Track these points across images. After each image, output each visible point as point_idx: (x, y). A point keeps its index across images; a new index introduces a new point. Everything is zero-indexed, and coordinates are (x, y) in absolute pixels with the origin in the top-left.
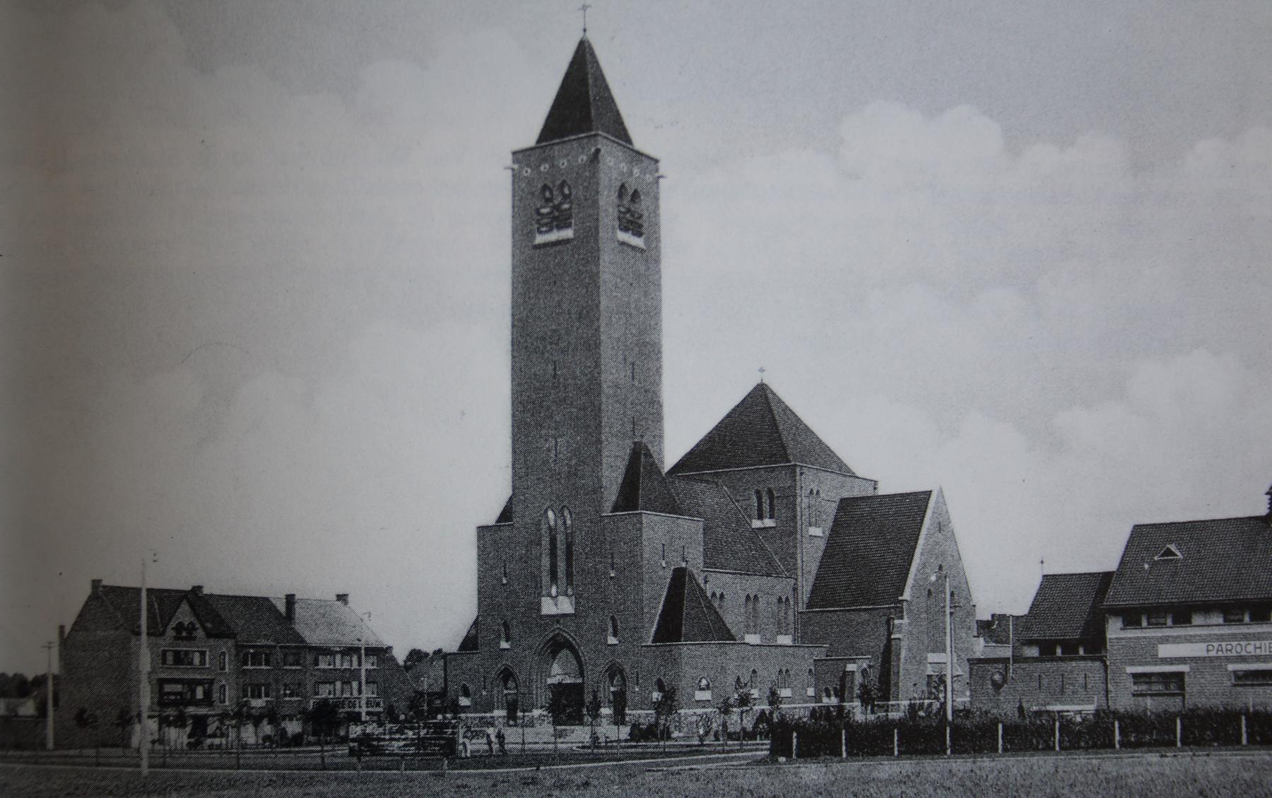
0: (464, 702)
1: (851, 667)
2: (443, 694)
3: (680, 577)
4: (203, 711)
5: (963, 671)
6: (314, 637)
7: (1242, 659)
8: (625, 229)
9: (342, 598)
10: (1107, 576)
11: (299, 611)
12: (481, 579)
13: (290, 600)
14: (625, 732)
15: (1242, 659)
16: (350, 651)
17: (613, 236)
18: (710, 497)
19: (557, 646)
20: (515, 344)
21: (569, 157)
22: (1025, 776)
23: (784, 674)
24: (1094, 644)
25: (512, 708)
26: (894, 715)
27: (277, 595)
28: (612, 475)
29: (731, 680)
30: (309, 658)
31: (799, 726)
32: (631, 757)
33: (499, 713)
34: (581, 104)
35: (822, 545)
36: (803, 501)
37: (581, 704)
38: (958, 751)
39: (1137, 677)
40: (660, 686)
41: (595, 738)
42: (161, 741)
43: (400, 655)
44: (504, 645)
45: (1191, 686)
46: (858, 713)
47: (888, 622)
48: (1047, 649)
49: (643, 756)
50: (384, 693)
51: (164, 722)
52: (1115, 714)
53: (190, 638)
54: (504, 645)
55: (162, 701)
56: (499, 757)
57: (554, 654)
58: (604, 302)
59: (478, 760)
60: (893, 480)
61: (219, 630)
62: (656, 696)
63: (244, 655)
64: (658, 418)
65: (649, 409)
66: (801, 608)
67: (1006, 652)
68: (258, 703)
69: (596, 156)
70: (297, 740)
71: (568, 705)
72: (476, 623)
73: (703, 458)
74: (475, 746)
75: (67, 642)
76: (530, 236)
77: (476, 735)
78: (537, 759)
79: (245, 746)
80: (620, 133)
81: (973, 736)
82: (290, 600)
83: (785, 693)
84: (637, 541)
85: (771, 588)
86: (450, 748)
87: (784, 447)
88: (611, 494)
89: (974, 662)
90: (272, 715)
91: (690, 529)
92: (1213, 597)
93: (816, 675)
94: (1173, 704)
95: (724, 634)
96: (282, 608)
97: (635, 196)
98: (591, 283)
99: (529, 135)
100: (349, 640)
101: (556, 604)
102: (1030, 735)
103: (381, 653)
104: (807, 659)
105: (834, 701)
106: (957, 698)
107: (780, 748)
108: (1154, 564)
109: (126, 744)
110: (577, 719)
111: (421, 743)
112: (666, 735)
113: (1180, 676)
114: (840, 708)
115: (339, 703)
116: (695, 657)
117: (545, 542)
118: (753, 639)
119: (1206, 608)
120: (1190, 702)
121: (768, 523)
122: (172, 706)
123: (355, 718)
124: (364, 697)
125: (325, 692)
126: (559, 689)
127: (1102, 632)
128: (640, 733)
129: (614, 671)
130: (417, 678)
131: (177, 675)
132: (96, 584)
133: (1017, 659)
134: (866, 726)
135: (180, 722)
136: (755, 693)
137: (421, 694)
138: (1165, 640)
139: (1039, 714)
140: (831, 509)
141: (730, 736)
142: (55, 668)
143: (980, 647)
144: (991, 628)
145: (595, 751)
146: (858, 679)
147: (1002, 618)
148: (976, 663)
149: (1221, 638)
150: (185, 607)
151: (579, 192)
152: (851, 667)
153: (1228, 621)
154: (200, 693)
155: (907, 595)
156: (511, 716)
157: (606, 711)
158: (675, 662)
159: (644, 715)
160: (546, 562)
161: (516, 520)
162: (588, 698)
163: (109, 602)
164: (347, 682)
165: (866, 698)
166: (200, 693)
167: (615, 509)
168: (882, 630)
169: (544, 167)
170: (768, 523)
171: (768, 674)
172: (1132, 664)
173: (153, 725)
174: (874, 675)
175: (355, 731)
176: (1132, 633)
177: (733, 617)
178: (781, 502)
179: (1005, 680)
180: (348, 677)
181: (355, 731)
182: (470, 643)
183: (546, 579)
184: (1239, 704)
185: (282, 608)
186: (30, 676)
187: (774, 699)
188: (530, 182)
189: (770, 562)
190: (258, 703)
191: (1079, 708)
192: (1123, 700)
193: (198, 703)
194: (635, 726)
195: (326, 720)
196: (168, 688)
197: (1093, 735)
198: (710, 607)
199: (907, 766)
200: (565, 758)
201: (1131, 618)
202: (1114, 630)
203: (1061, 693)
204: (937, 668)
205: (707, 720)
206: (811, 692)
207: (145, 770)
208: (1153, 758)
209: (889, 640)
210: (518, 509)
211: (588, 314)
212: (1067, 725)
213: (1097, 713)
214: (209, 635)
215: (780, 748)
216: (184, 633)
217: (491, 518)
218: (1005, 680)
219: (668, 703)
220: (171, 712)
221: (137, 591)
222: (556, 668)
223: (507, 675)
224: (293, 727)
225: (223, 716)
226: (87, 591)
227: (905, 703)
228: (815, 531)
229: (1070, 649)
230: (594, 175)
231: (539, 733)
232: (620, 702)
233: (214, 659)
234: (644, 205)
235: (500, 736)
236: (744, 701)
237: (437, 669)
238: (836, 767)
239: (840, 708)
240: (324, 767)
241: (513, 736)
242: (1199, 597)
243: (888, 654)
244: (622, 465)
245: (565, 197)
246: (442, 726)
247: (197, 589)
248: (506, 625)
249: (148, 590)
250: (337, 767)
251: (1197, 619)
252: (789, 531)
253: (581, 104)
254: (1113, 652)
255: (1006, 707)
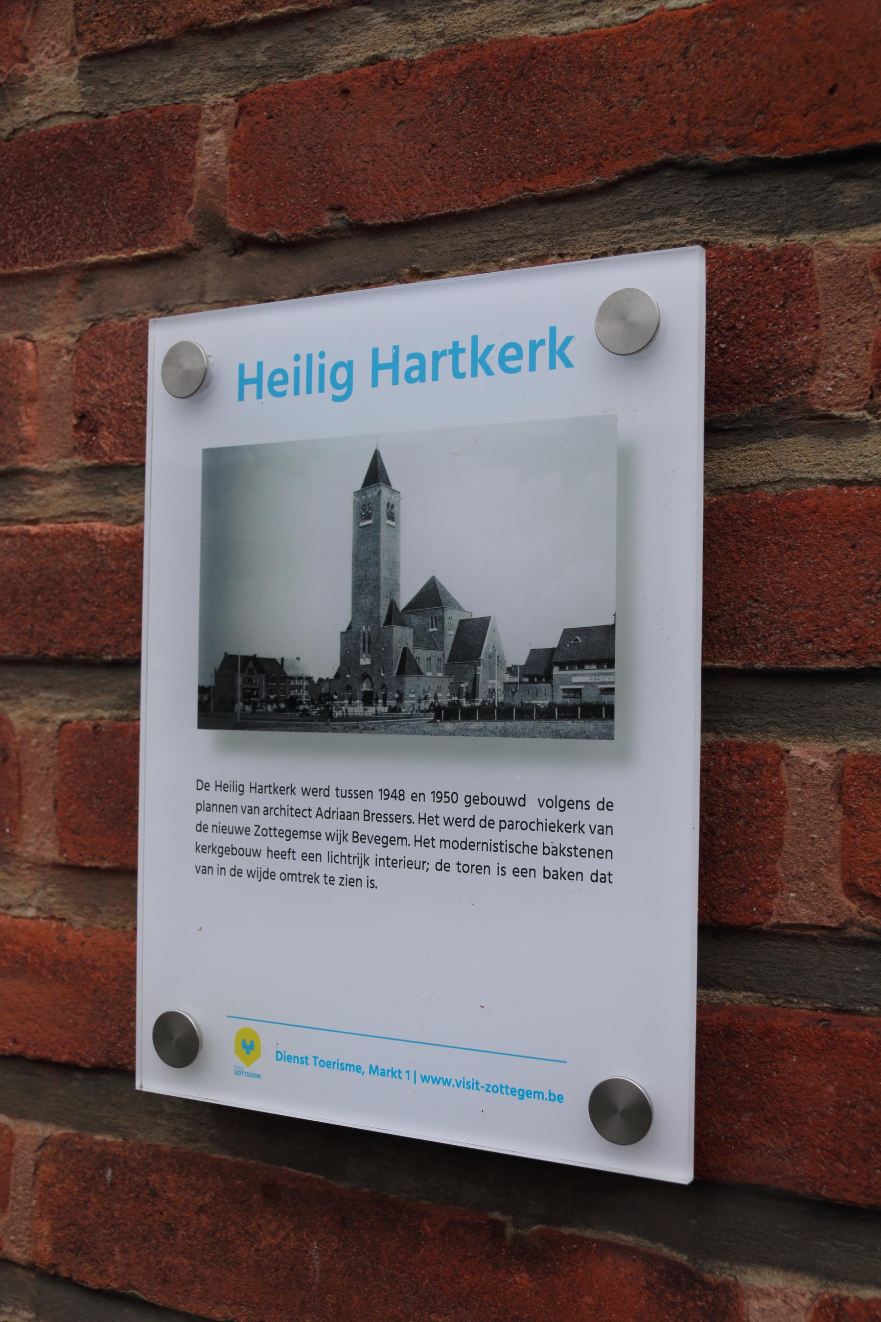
0: (335, 697)
1: (462, 685)
2: (329, 694)
3: (405, 650)
4: (256, 699)
5: (501, 687)
6: (290, 673)
7: (603, 683)
8: (389, 519)
9: (298, 659)
10: (553, 650)
11: (285, 664)
12: (341, 652)
13: (282, 659)
14: (386, 709)
15: (603, 683)
16: (300, 678)
17: (385, 521)
18: (416, 620)
19: (365, 677)
20: (353, 564)
21: (371, 493)
22: (523, 729)
23: (439, 688)
24: (548, 677)
25: (351, 699)
26: (477, 704)
27: (278, 658)
28: (383, 612)
29: (422, 690)
30: (288, 681)
31: (444, 708)
32: (388, 719)
33: (346, 701)
34: (376, 474)
35: (453, 638)
36: (446, 621)
37: (372, 698)
38: (499, 719)
39: (564, 690)
40: (398, 692)
41: (377, 711)
42: (244, 710)
43: (316, 680)
44: (348, 676)
45: (584, 695)
46: (465, 703)
47: (475, 668)
48: (531, 679)
49: (392, 718)
50: (310, 694)
51: (245, 703)
52: (556, 705)
53: (253, 673)
54: (348, 676)
55: (244, 695)
56: (346, 718)
57: (364, 680)
58: (382, 547)
59: (340, 719)
60: (476, 615)
61: (261, 671)
62: (397, 696)
63: (268, 681)
64: (398, 590)
65: (395, 587)
66: (446, 662)
67: (517, 680)
68: (272, 697)
69: (379, 493)
70: (284, 711)
71: (369, 699)
72: (339, 668)
73: (416, 605)
74: (338, 714)
75: (218, 674)
76: (358, 523)
77: (339, 709)
78: (358, 719)
79: (268, 712)
80: (388, 483)
81: (505, 713)
82: (282, 659)
83: (439, 695)
84: (391, 637)
85: (435, 654)
86: (330, 714)
87: (440, 600)
88: (383, 620)
89: (505, 684)
90: (277, 701)
91: (408, 632)
92: (593, 658)
93: (450, 688)
94: (577, 701)
95: (419, 672)
96: (280, 662)
97: (393, 506)
98: (377, 539)
99: (358, 486)
100: (300, 674)
101: (365, 661)
102: (525, 713)
103: (309, 679)
104: (447, 682)
105: (456, 698)
106: (499, 698)
107: (438, 717)
108: (571, 644)
109: (232, 710)
110: (370, 704)
111: (321, 712)
112: (400, 711)
113: (579, 691)
114: (458, 701)
115: (297, 697)
116: (410, 681)
117: (362, 638)
118: (429, 674)
119: (590, 662)
120: (584, 700)
121: (435, 629)
122: (247, 698)
123: (301, 703)
124: (304, 695)
125: (292, 693)
126: (365, 693)
127: (551, 671)
128: (392, 710)
129: (383, 686)
130: (321, 688)
131: (248, 686)
132: (226, 654)
133: (521, 682)
134: (467, 708)
135: (249, 703)
136: (430, 695)
137: (321, 694)
138: (575, 675)
139: (528, 704)
140: (456, 624)
141: (422, 711)
142: (213, 684)
143: (508, 678)
144: (511, 671)
145: (377, 717)
146: (465, 690)
147: (515, 666)
148: (506, 685)
149: (595, 674)
150: (251, 662)
151: (374, 506)
152: (462, 685)
153: (598, 668)
154: (255, 693)
155: (482, 657)
156: (350, 703)
157: (380, 701)
158: (402, 683)
159: (393, 703)
160: (362, 645)
161: (353, 630)
162: (374, 696)
163: (230, 660)
164: (299, 690)
165: (467, 698)
166: (255, 693)
167: (385, 625)
168: (473, 671)
169: (363, 497)
170: (435, 629)
171: (434, 688)
172: (562, 684)
173: (241, 704)
174: (470, 689)
175: (302, 707)
176: (562, 672)
177: (422, 666)
178: (439, 621)
179: (516, 691)
180: (300, 688)
181: (302, 707)
182: (337, 676)
183: (361, 651)
184: (602, 702)
185: (280, 662)
186: (206, 686)
187: (436, 697)
188: (358, 503)
189: (435, 645)
190: (272, 697)
191: (542, 702)
192: (559, 700)
193: (255, 697)
194: (390, 707)
195: (293, 703)
196: (247, 691)
197: (547, 714)
198: (415, 662)
199: (481, 724)
200: (366, 718)
201: (562, 667)
202: (556, 671)
203: (536, 696)
204: (492, 685)
205: (413, 705)
206: (448, 695)
207: (239, 720)
208: (569, 723)
209: (476, 675)
210: (353, 625)
211: (376, 552)
212: (538, 709)
213: (550, 704)
214: (258, 672)
215: (438, 717)
216: (251, 671)
217: (344, 629)
218: (516, 691)
219: (400, 699)
220: (247, 700)
221: (236, 656)
222: (364, 685)
223: (349, 688)
224: (283, 706)
225: (262, 702)
226: (221, 657)
227: (481, 700)
228: (451, 632)
229: (540, 678)
230: (379, 499)
231: (358, 709)
232: (385, 698)
233: (259, 680)
234: (395, 510)
235: (346, 710)
236: (426, 698)
237: (327, 685)
238: (457, 724)
239: (458, 701)
240: (292, 720)
241: (351, 710)
242: (588, 658)
243: (475, 681)
244: (387, 608)
245: (370, 508)
246: (328, 706)
247: (255, 656)
248: (349, 669)
249: (242, 656)
250: (296, 721)
251: (587, 667)
252: (442, 632)
253: (376, 474)
254: (556, 680)
255: (517, 702)
